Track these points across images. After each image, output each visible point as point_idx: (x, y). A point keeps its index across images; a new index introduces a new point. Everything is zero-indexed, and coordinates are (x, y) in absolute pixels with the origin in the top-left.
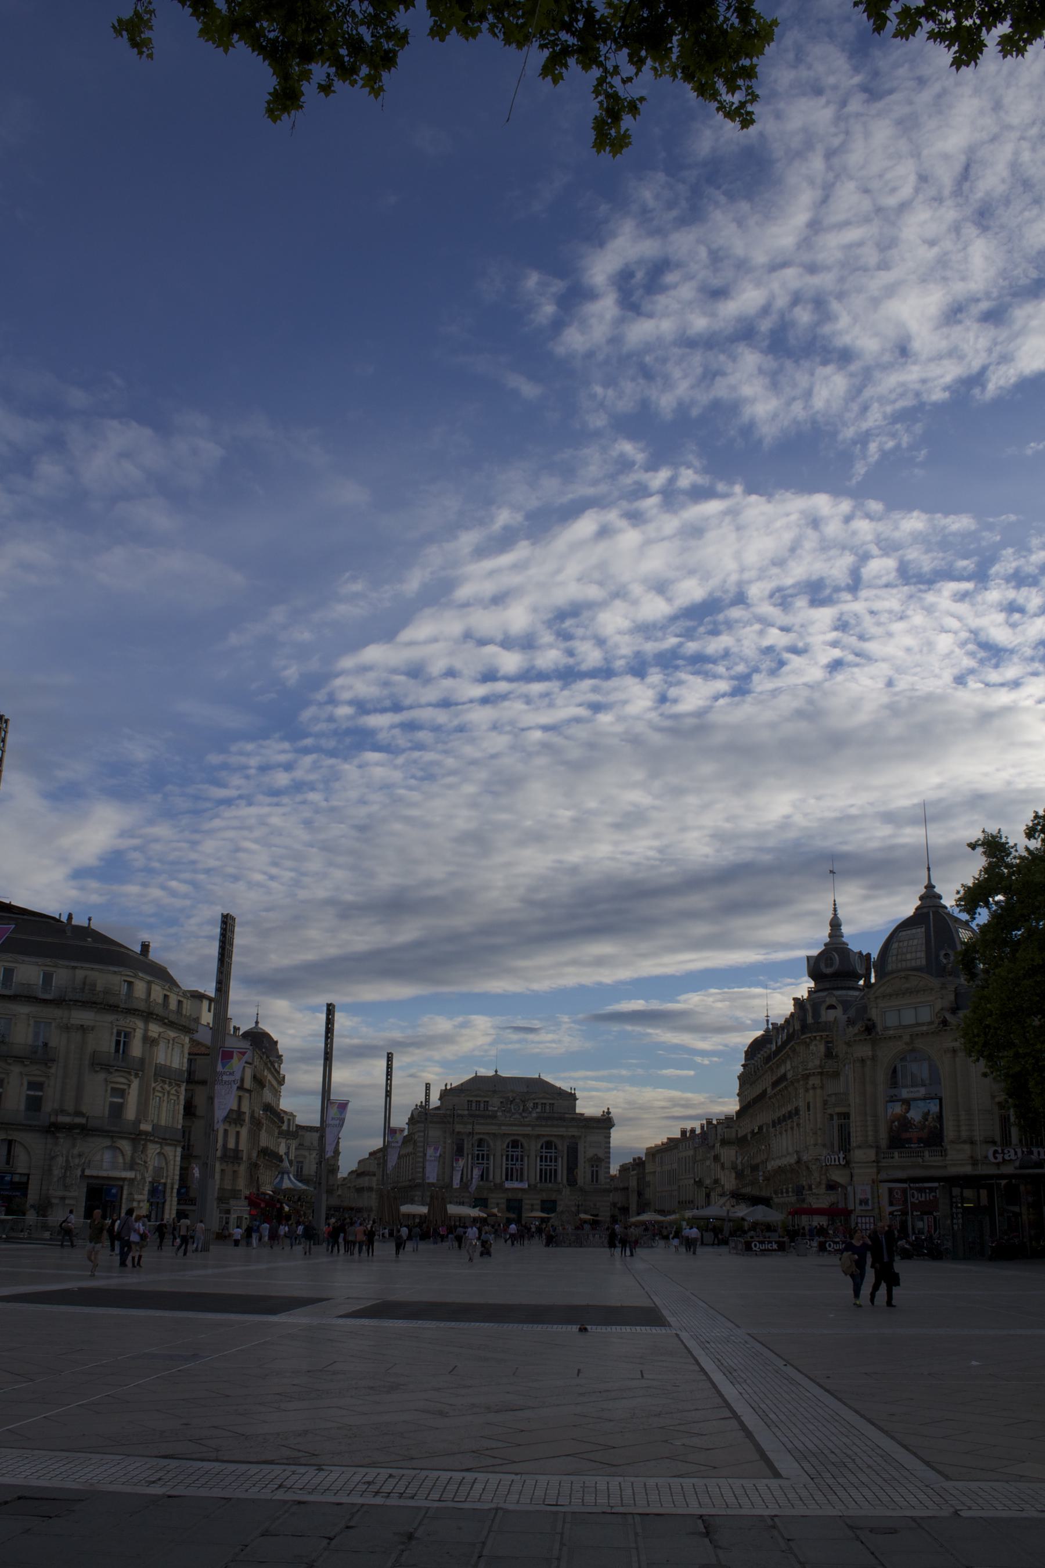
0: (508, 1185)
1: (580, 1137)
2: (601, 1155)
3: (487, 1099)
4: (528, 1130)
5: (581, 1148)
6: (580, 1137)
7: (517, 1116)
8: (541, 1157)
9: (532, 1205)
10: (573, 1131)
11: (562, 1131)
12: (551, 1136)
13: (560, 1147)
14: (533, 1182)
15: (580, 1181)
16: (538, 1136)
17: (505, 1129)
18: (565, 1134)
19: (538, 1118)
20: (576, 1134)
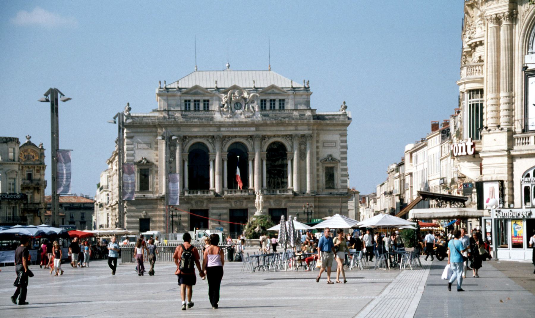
1: (311, 136)
3: (206, 98)
12: (279, 136)
20: (306, 132)
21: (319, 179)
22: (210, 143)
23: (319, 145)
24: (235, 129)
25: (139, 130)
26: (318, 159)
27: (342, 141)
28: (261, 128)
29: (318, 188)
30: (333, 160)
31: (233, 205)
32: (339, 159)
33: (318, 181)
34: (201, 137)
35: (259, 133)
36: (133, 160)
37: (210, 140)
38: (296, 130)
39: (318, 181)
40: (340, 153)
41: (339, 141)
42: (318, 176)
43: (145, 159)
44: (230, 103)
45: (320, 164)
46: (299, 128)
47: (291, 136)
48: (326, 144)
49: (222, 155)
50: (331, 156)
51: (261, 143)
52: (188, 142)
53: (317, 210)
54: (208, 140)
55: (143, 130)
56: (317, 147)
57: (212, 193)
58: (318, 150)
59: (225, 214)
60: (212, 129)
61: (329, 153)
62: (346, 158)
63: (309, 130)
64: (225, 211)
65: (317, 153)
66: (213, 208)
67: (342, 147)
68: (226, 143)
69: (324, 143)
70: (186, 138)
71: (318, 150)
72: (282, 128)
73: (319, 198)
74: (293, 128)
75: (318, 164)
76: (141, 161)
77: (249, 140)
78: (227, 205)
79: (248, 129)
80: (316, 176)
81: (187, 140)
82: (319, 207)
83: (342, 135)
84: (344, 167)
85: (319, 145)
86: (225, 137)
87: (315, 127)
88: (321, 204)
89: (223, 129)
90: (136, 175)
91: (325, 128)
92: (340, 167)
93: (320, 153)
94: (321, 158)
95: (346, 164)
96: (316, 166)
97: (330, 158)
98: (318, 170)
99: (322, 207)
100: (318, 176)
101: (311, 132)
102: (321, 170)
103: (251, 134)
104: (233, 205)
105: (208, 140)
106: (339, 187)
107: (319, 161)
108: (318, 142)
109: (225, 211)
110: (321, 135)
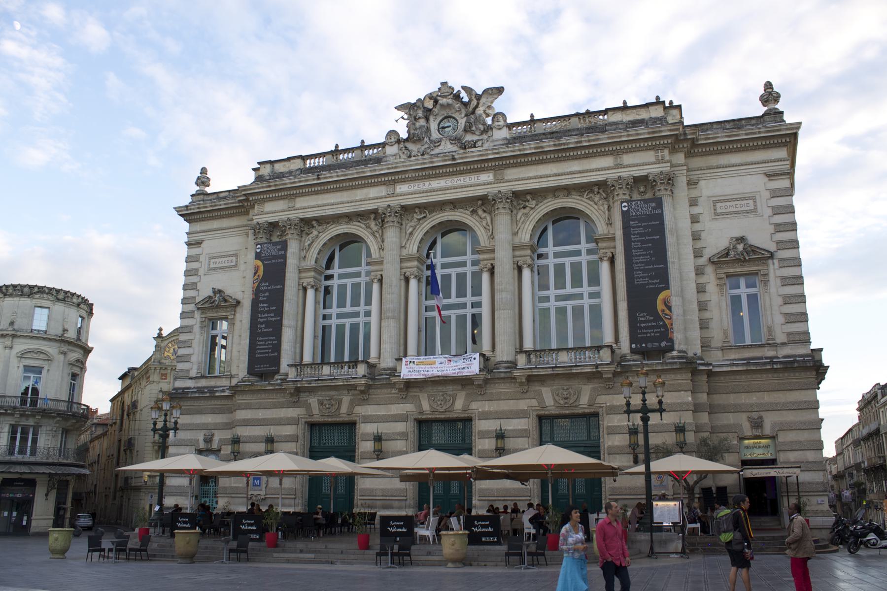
0: (408, 371)
2: (761, 236)
4: (482, 183)
5: (676, 216)
6: (670, 180)
7: (447, 147)
8: (541, 273)
9: (500, 436)
10: (642, 163)
11: (599, 168)
12: (568, 190)
13: (601, 228)
14: (504, 353)
15: (686, 338)
16: (519, 198)
17: (409, 192)
18: (611, 175)
19: (509, 142)
20: (653, 170)
21: (707, 315)
22: (373, 234)
23: (696, 210)
24: (436, 184)
25: (215, 224)
26: (698, 254)
27: (775, 194)
28: (511, 173)
29: (705, 345)
30: (754, 249)
31: (426, 406)
32: (772, 247)
33: (704, 325)
34: (349, 217)
35: (505, 187)
36: (194, 298)
37: (372, 224)
38: (618, 166)
39: (704, 325)
40: (771, 229)
41: (767, 194)
42: (703, 307)
43: (220, 291)
44: (427, 119)
45: (709, 270)
46: (627, 159)
47: (602, 185)
48: (721, 207)
49: (402, 261)
50: (742, 239)
51: (514, 221)
52: (317, 236)
53: (704, 418)
54: (368, 227)
55: (225, 223)
56: (695, 219)
57: (362, 370)
58: (698, 227)
59: (404, 436)
60: (373, 192)
61: (738, 234)
62: (794, 244)
63: (659, 161)
64: (400, 427)
65: (696, 237)
66: (368, 419)
67: (778, 211)
68: (414, 228)
69: (715, 202)
70: (313, 227)
71: (698, 227)
72: (575, 166)
73: (710, 374)
74: (607, 161)
75: (699, 271)
76: (210, 297)
77: (480, 212)
78: (407, 408)
79: (473, 179)
80: (695, 306)
81: (315, 233)
82: (712, 410)
83: (770, 176)
84: (791, 272)
85: (696, 210)
86: (407, 210)
87: (680, 158)
88: (720, 399)
89: (402, 188)
90: (198, 336)
91: (714, 160)
92: (774, 270)
93: (703, 235)
94: (709, 252)
95: (797, 262)
96: (693, 274)
97: (740, 247)
98: (701, 289)
99: (726, 409)
100: (703, 307)
101: (665, 168)
102: (712, 288)
103: (480, 192)
104: (426, 406)
105: (368, 227)
106: (780, 338)
107: (702, 261)
108: (693, 203)
109: (400, 427)
110: (702, 183)
